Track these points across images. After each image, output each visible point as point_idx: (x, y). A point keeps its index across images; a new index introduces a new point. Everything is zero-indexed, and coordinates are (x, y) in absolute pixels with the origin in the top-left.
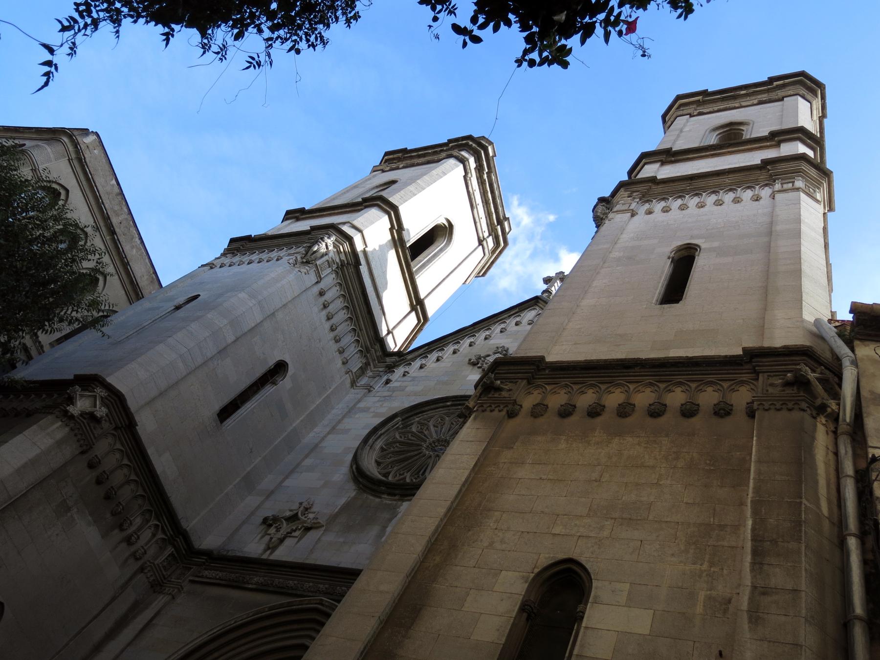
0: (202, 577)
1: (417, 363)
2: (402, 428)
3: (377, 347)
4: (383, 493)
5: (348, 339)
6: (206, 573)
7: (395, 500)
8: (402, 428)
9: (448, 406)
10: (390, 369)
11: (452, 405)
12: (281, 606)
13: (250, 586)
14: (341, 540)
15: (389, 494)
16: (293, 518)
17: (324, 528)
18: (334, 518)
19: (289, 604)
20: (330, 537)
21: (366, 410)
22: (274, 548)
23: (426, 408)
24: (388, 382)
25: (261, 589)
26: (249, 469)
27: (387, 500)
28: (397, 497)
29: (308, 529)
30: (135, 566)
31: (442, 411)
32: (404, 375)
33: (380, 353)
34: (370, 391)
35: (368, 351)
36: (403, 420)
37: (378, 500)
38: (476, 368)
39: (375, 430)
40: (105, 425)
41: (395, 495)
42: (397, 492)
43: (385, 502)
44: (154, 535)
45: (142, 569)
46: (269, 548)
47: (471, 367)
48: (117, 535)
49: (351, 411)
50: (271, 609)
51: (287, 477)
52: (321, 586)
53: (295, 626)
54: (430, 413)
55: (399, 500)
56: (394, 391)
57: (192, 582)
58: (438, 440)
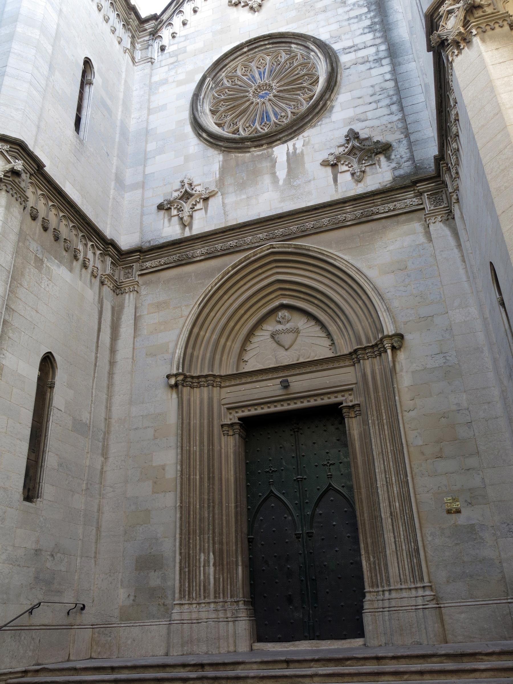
0: (147, 268)
1: (177, 20)
2: (216, 87)
3: (133, 16)
4: (250, 148)
5: (113, 16)
6: (148, 264)
7: (264, 150)
8: (216, 87)
9: (245, 52)
10: (154, 34)
11: (249, 51)
12: (240, 262)
13: (198, 259)
14: (244, 197)
15: (256, 147)
16: (187, 196)
17: (219, 193)
18: (221, 182)
19: (246, 258)
20: (231, 199)
21: (164, 82)
22: (190, 225)
23: (227, 61)
24: (163, 49)
25: (210, 257)
26: (114, 171)
27: (256, 152)
28: (265, 147)
29: (206, 200)
30: (97, 282)
31: (243, 58)
32: (174, 37)
33: (137, 22)
34: (152, 63)
35: (128, 23)
36: (212, 79)
37: (248, 155)
38: (240, 6)
39: (196, 96)
40: (24, 176)
41: (262, 145)
42: (264, 142)
43: (255, 154)
44: (94, 254)
45: (102, 283)
46: (185, 226)
47: (234, 9)
48: (77, 265)
49: (151, 88)
50: (234, 267)
51: (145, 166)
52: (261, 235)
53: (260, 271)
54: (233, 65)
56: (177, 56)
57: (140, 275)
58: (259, 86)
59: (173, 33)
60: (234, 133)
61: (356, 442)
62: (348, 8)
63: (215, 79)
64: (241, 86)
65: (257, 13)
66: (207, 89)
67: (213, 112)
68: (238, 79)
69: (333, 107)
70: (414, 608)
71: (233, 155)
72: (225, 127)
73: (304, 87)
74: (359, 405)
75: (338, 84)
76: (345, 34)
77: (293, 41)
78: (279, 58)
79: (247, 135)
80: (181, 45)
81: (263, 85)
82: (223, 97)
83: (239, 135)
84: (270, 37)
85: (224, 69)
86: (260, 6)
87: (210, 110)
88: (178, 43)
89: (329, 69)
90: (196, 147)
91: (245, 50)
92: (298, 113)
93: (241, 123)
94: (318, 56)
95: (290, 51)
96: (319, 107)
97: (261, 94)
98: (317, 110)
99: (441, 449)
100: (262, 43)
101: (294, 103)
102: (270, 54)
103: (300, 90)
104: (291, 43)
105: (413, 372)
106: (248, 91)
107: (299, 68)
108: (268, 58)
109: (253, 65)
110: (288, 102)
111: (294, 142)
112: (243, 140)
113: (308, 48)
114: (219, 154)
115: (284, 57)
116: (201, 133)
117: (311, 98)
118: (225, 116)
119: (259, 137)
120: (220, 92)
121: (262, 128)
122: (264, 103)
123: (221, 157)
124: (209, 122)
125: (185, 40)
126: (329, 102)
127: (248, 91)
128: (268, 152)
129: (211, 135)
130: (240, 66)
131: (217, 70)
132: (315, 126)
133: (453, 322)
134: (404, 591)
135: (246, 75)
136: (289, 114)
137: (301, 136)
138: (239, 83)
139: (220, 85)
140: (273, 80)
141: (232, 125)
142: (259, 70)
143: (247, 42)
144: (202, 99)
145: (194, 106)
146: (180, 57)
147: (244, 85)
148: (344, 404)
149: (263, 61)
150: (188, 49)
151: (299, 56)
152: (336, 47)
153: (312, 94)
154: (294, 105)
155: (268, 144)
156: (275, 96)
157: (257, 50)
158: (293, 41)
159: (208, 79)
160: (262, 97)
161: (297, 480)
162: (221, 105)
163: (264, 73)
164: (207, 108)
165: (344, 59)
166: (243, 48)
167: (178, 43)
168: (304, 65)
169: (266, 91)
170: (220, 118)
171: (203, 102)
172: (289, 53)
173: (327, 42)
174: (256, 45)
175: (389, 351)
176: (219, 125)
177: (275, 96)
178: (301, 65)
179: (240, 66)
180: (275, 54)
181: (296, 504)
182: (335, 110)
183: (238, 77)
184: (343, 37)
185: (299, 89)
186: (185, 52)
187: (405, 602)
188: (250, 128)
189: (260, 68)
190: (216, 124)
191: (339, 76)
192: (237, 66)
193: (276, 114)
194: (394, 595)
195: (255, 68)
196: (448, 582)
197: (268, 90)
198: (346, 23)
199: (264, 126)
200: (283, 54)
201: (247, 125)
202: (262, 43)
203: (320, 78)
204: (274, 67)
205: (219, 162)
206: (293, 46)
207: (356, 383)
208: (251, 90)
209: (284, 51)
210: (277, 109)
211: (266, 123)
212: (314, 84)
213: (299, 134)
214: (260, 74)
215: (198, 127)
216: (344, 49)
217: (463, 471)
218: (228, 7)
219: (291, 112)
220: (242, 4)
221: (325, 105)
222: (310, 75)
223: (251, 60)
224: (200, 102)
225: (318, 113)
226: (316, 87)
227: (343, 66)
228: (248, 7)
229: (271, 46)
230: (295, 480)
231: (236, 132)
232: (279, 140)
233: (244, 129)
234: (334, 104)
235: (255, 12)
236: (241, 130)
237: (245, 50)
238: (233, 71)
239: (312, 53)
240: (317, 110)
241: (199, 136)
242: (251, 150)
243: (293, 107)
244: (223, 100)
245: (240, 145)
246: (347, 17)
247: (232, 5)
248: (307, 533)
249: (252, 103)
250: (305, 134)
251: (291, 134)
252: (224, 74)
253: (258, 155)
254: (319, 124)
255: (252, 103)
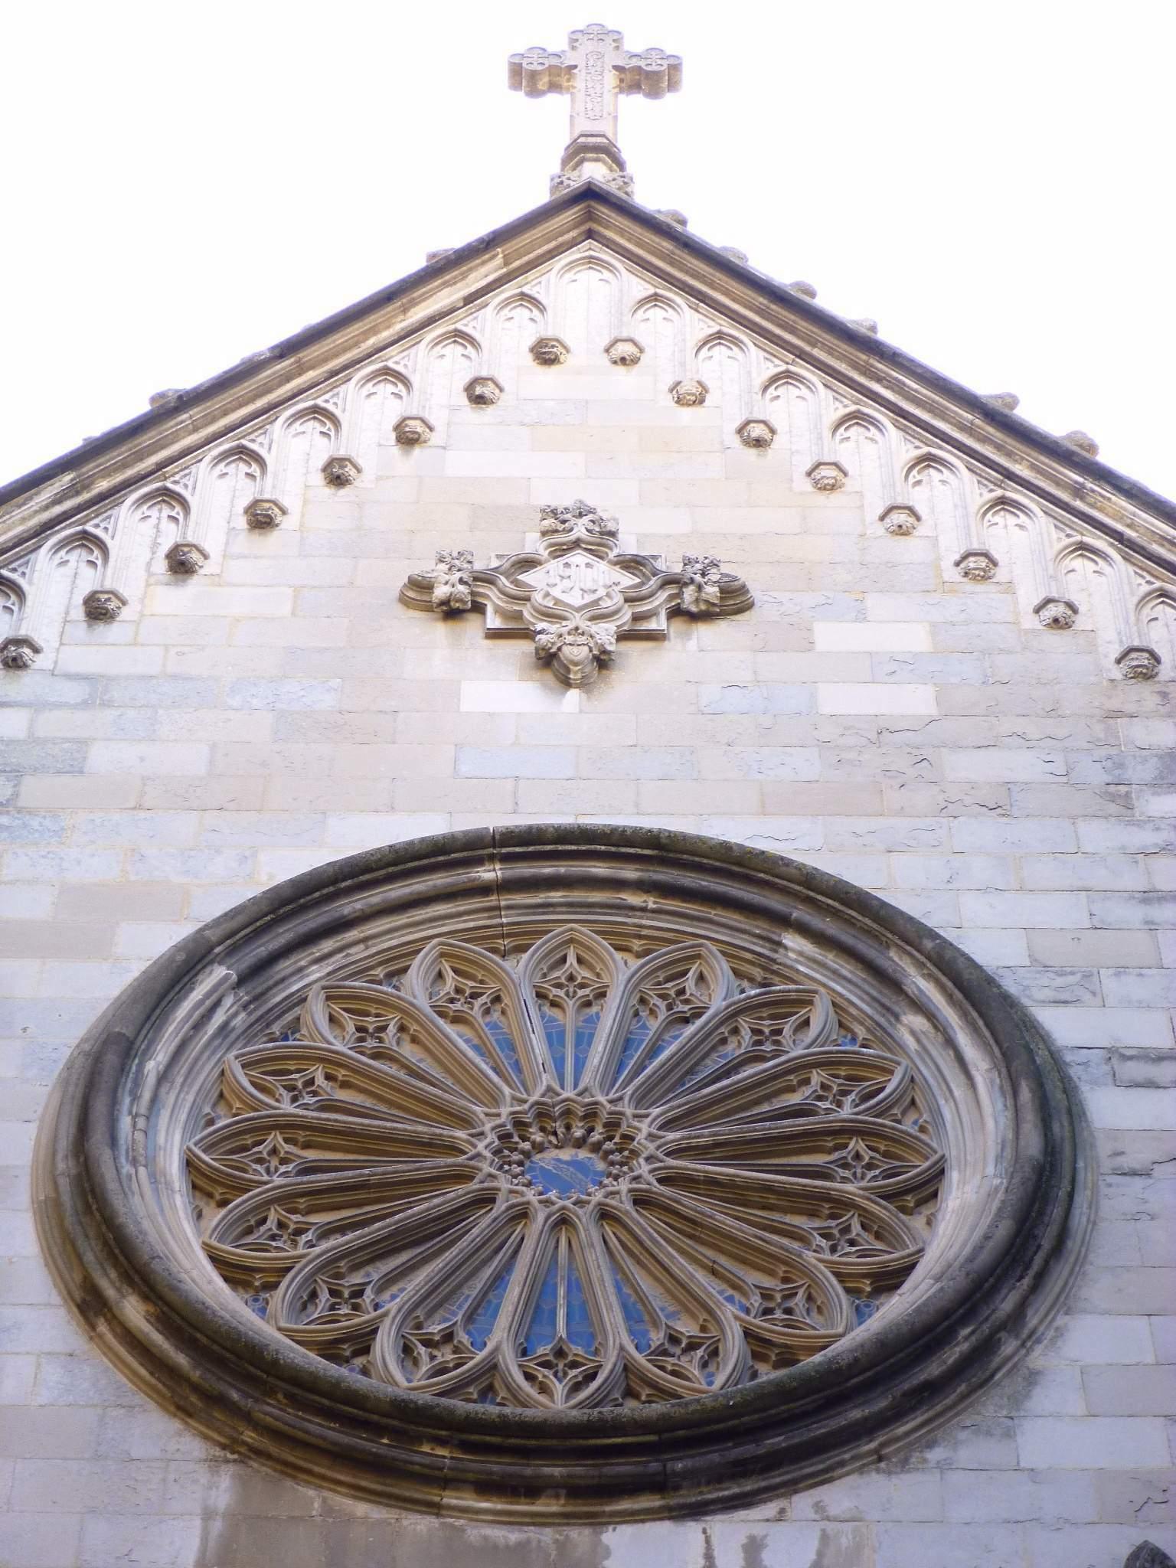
2: (249, 1033)
4: (447, 1482)
8: (249, 1033)
9: (485, 889)
15: (486, 1487)
31: (465, 915)
36: (242, 981)
37: (420, 1524)
38: (472, 627)
41: (531, 1490)
42: (556, 1471)
43: (477, 1533)
47: (441, 630)
55: (567, 1519)
58: (543, 1113)
59: (19, 642)
60: (329, 1349)
62: (1148, 838)
63: (259, 985)
64: (413, 1073)
65: (573, 694)
66: (198, 1026)
67: (204, 1183)
68: (402, 1029)
69: (1033, 1378)
71: (312, 1498)
72: (279, 1299)
73: (840, 1205)
75: (1072, 1245)
76: (1121, 970)
77: (800, 912)
78: (690, 983)
79: (425, 1398)
80: (51, 724)
81: (567, 1113)
82: (287, 1107)
83: (365, 1372)
84: (662, 851)
85: (327, 945)
86: (602, 661)
87: (190, 1165)
88: (38, 706)
89: (1033, 1144)
90: (53, 1374)
91: (488, 873)
92: (787, 1357)
93: (395, 1302)
94: (950, 1043)
95: (768, 965)
96: (952, 1354)
97: (546, 1159)
98: (933, 1369)
100: (600, 869)
101: (767, 1282)
102: (637, 945)
103: (813, 1214)
104: (784, 921)
106: (464, 1120)
107: (817, 1077)
108: (621, 971)
109: (519, 969)
110: (723, 1260)
111: (758, 1530)
112: (408, 1420)
113: (892, 983)
114: (213, 1463)
115: (720, 991)
116: (110, 1293)
117: (889, 1280)
118: (281, 1225)
119: (504, 1426)
120: (271, 1068)
121: (529, 1377)
122: (563, 1221)
123: (221, 1488)
124: (182, 1239)
125: (85, 704)
126: (1009, 1347)
127: (464, 1120)
128: (562, 1546)
129: (180, 1317)
130: (430, 951)
131: (284, 934)
132: (904, 1464)
135: (457, 1019)
136: (734, 1346)
137: (802, 1503)
138: (408, 1051)
139: (276, 1028)
140: (642, 1099)
141: (324, 1296)
142: (555, 1013)
143: (509, 837)
144: (151, 1080)
145: (100, 1106)
146: (33, 790)
147: (428, 1066)
149: (583, 973)
150: (101, 758)
151: (820, 1015)
152: (1065, 1027)
153: (893, 1257)
154: (766, 1295)
155: (575, 1491)
156: (642, 1201)
157: (556, 896)
158: (800, 912)
159: (219, 972)
160: (551, 1179)
162: (263, 1149)
163: (584, 1040)
164: (172, 1142)
165: (1110, 1110)
166: (479, 861)
167: (38, 706)
168: (852, 1070)
169: (583, 1154)
170: (247, 1226)
171: (154, 1099)
172: (758, 973)
173: (1010, 985)
174: (562, 868)
176: (235, 1274)
177: (642, 1201)
178: (826, 1063)
179: (430, 951)
180: (665, 953)
182: (1042, 1399)
183: (407, 1012)
184: (1110, 984)
185: (810, 1203)
186: (77, 769)
188: (446, 1355)
189: (554, 1004)
190: (216, 1260)
191: (1081, 1199)
192: (411, 951)
193: (636, 1313)
195: (528, 994)
197: (596, 1148)
198: (1135, 914)
199: (546, 1365)
200: (720, 970)
201: (435, 1328)
202: (600, 869)
203: (954, 1176)
204: (654, 1025)
205: (208, 1515)
206: (792, 941)
208: (491, 1118)
209: (730, 953)
210: (645, 1283)
211: (560, 1353)
212: (910, 1200)
213: (792, 1487)
214: (555, 1038)
215: (96, 1249)
216: (1115, 1054)
218: (400, 609)
219: (748, 1334)
220: (494, 621)
221: (986, 1348)
222: (890, 1145)
223: (519, 941)
224: (135, 1098)
225: (931, 1390)
226: (918, 1222)
227: (1104, 1148)
228: (526, 647)
229: (651, 902)
231: (347, 1350)
232: (658, 1485)
233: (407, 1350)
234: (1037, 1359)
235: (567, 683)
236: (385, 1346)
237: (488, 873)
238: (380, 972)
239: (918, 1022)
240: (933, 1369)
241: (90, 1306)
242: (451, 1499)
243: (756, 1301)
244: (288, 1127)
245: (383, 1446)
246: (1133, 880)
247: (428, 607)
249: (486, 1199)
250: (842, 1495)
251: (740, 1470)
252: (316, 973)
253: (491, 1549)
254: (935, 1455)
255: (486, 1199)
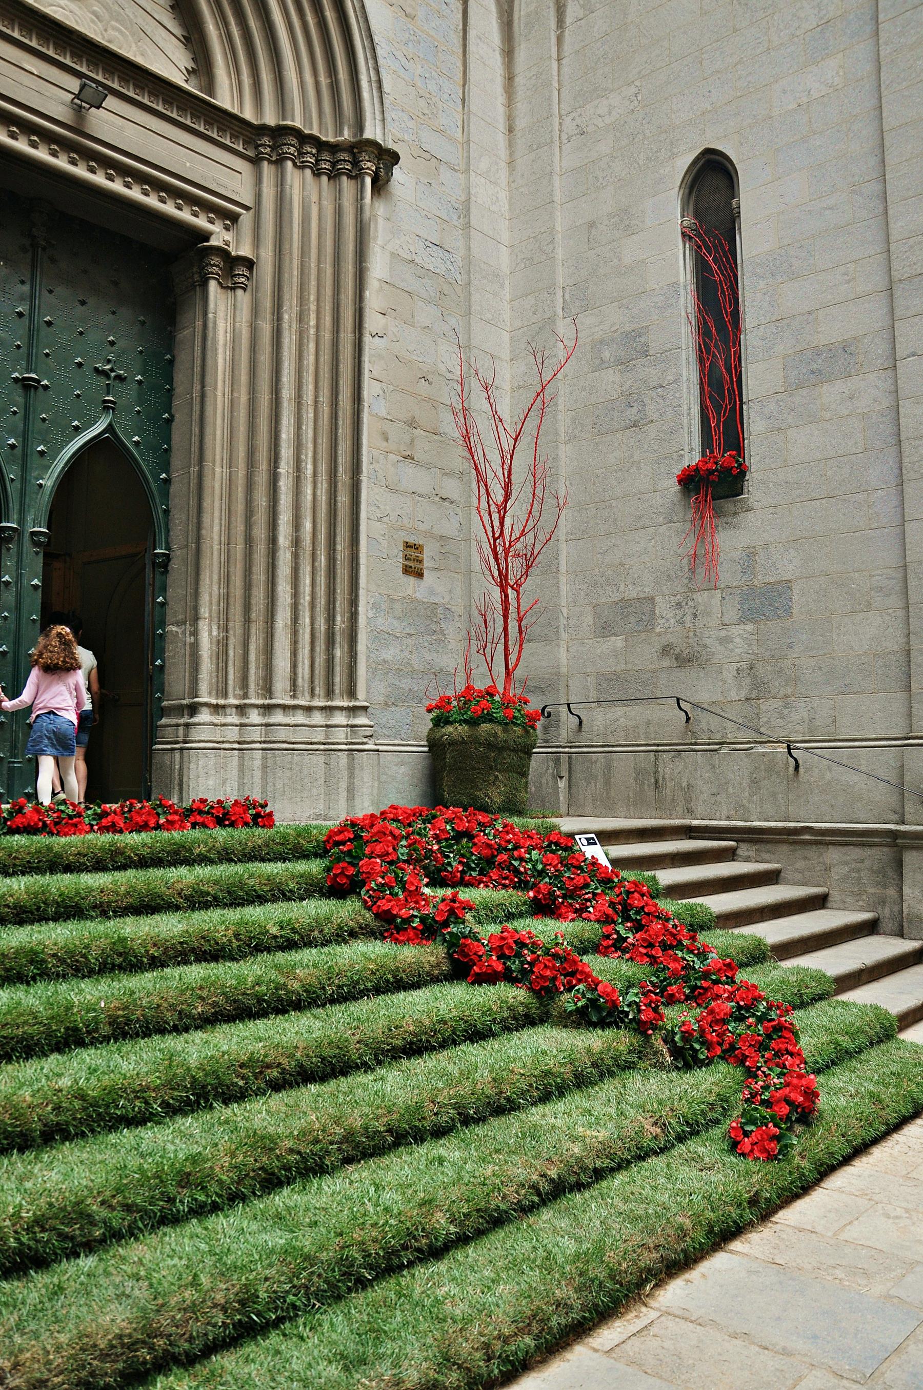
61: (220, 350)
70: (322, 747)
74: (249, 264)
99: (412, 441)
105: (392, 254)
133: (473, 198)
134: (337, 713)
148: (214, 242)
161: (27, 386)
175: (368, 181)
181: (13, 447)
187: (302, 735)
194: (278, 717)
196: (386, 704)
207: (247, 208)
217: (437, 499)
230: (16, 380)
248: (33, 534)
